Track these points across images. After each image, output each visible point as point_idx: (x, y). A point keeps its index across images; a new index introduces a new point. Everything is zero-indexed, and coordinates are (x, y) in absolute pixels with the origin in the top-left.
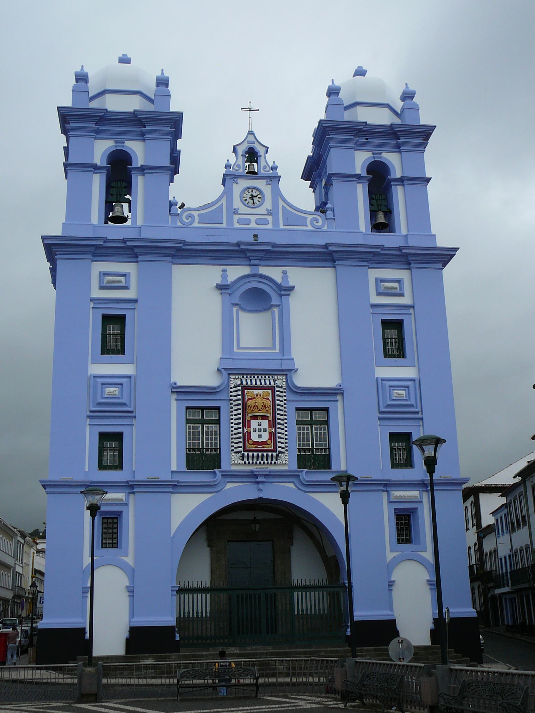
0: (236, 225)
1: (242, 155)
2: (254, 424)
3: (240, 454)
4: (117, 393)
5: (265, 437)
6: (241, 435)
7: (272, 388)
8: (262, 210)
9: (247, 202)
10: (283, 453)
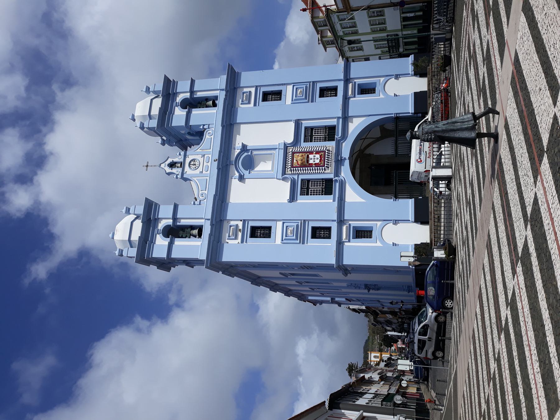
0: (209, 172)
1: (172, 169)
2: (311, 162)
3: (326, 168)
4: (291, 229)
5: (318, 156)
6: (316, 168)
7: (293, 153)
8: (201, 160)
9: (196, 167)
10: (326, 148)
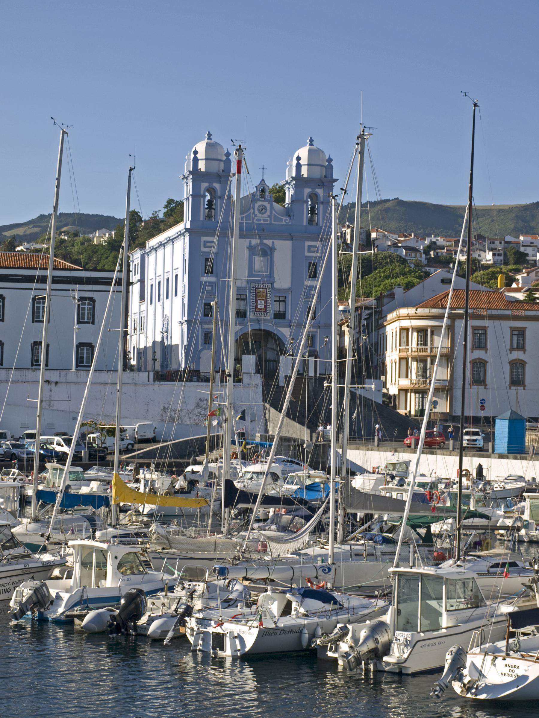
5: (263, 307)
8: (266, 215)
